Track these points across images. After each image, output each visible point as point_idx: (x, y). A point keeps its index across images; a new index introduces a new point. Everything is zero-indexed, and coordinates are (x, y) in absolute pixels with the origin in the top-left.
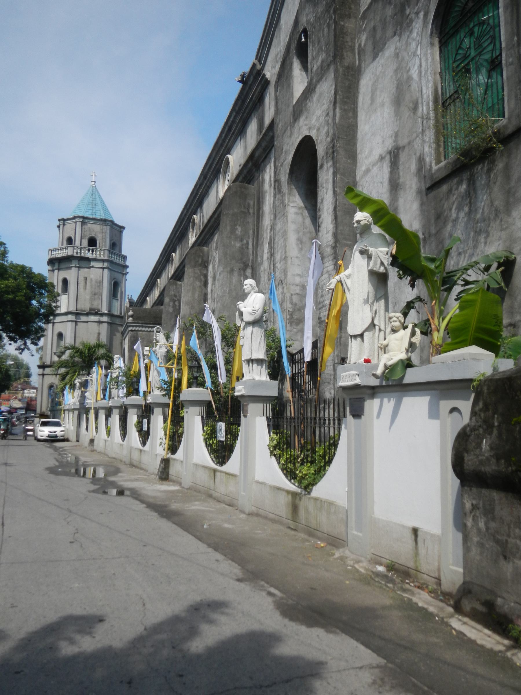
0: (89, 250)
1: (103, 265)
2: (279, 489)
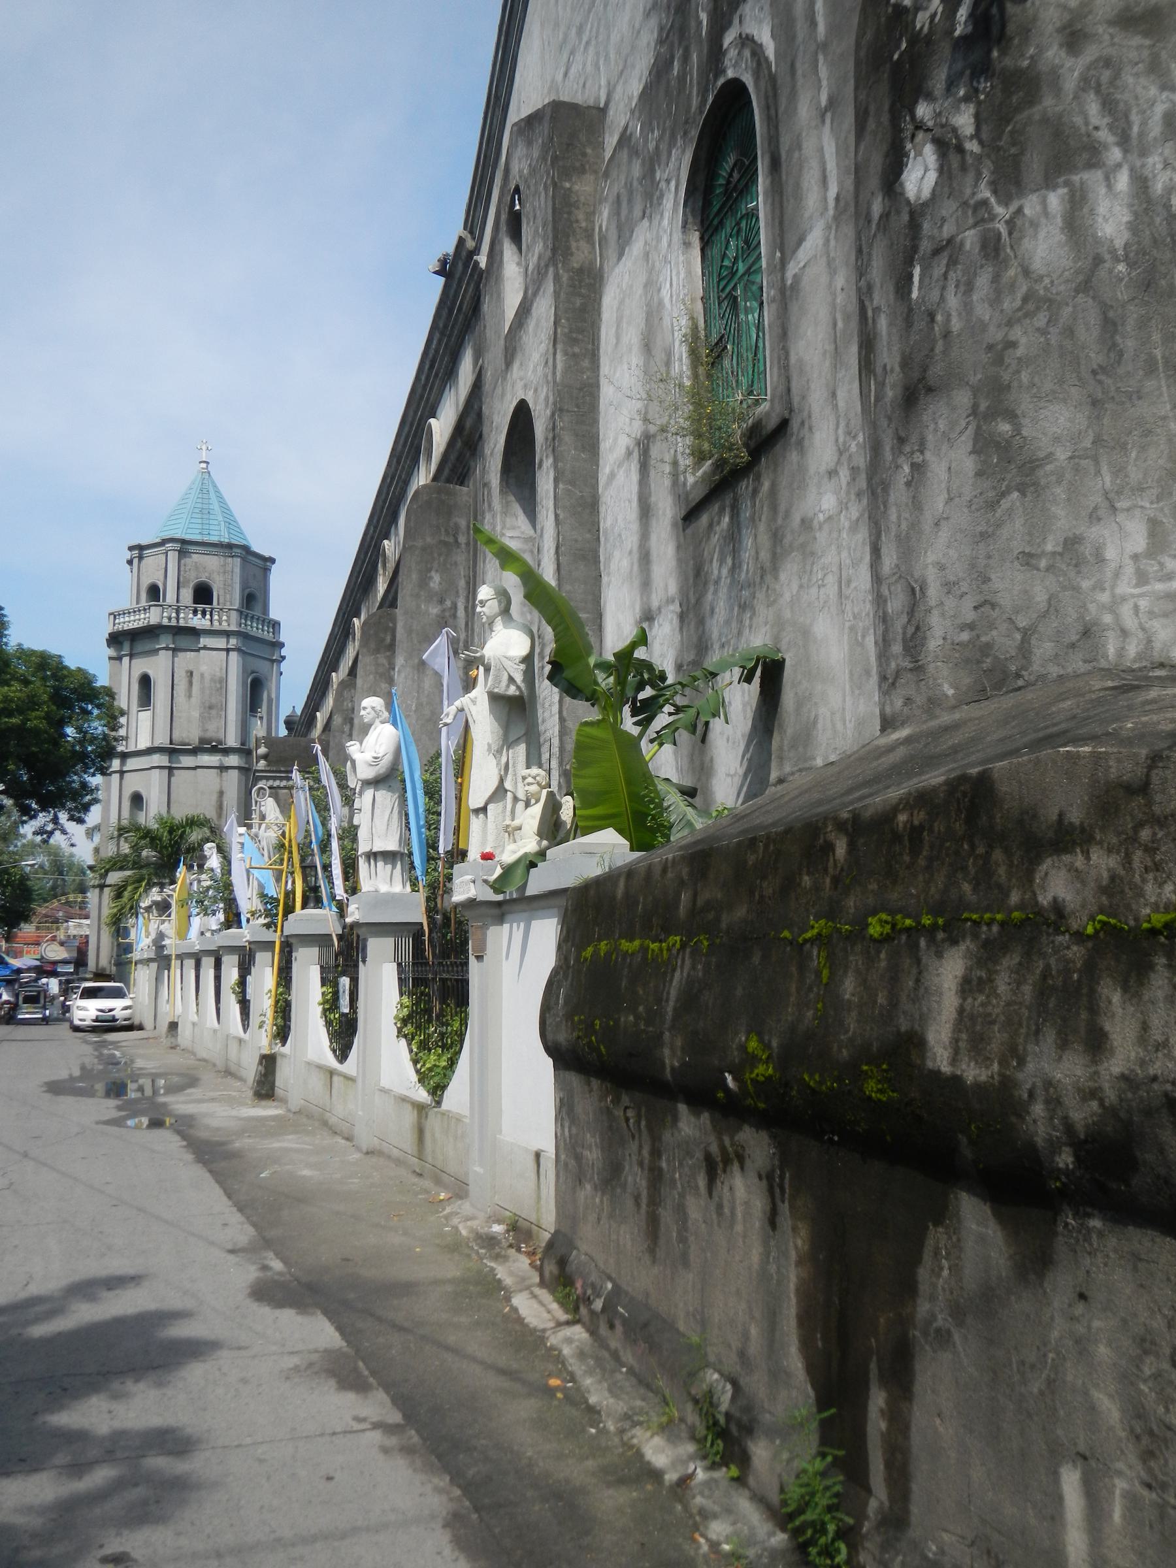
0: (195, 612)
1: (228, 642)
2: (404, 1099)
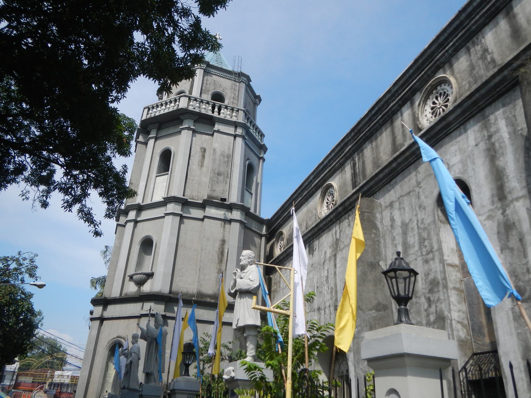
0: (213, 108)
1: (235, 131)
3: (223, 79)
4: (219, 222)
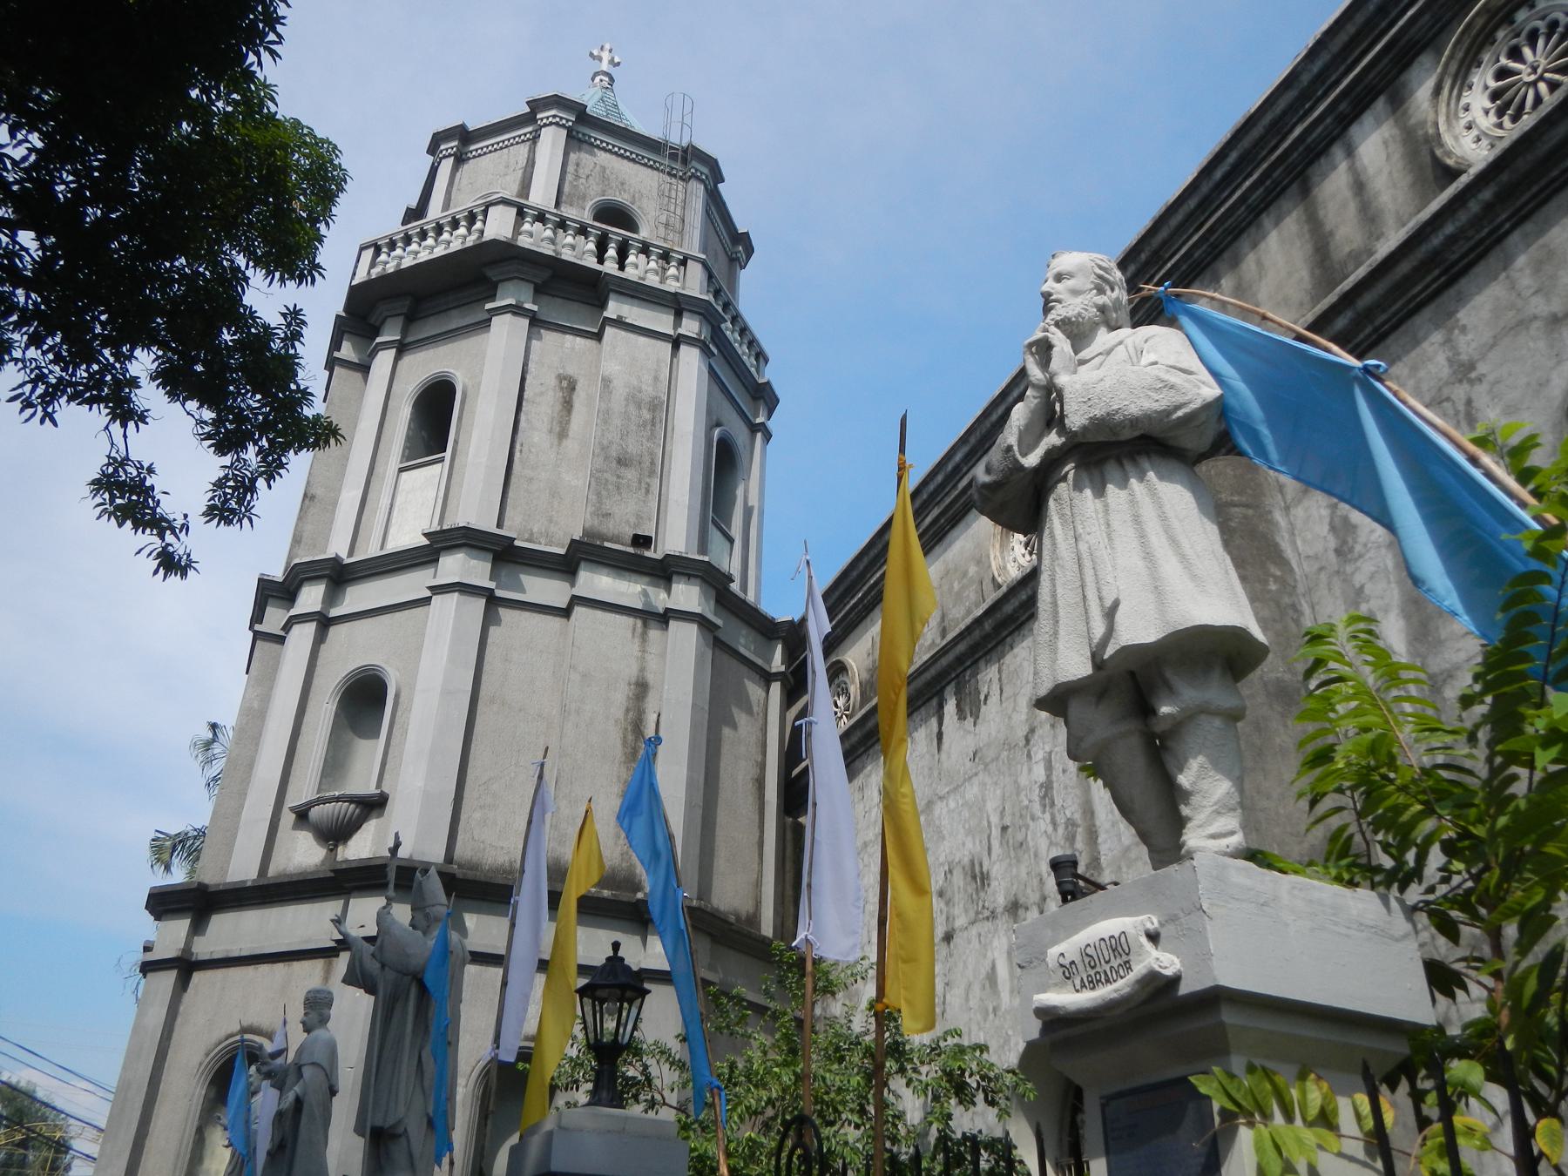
1: (677, 324)
3: (631, 164)
4: (626, 621)
